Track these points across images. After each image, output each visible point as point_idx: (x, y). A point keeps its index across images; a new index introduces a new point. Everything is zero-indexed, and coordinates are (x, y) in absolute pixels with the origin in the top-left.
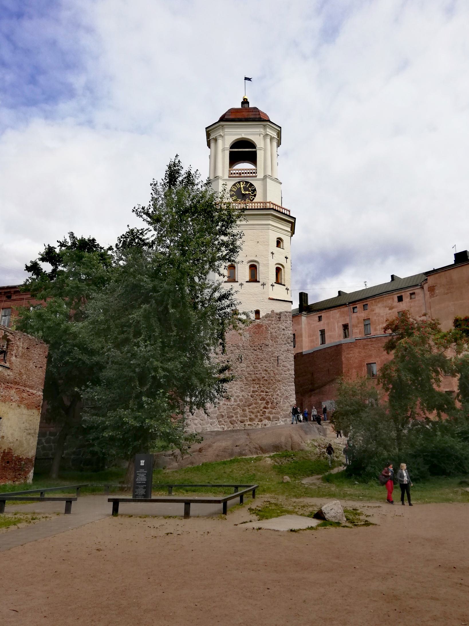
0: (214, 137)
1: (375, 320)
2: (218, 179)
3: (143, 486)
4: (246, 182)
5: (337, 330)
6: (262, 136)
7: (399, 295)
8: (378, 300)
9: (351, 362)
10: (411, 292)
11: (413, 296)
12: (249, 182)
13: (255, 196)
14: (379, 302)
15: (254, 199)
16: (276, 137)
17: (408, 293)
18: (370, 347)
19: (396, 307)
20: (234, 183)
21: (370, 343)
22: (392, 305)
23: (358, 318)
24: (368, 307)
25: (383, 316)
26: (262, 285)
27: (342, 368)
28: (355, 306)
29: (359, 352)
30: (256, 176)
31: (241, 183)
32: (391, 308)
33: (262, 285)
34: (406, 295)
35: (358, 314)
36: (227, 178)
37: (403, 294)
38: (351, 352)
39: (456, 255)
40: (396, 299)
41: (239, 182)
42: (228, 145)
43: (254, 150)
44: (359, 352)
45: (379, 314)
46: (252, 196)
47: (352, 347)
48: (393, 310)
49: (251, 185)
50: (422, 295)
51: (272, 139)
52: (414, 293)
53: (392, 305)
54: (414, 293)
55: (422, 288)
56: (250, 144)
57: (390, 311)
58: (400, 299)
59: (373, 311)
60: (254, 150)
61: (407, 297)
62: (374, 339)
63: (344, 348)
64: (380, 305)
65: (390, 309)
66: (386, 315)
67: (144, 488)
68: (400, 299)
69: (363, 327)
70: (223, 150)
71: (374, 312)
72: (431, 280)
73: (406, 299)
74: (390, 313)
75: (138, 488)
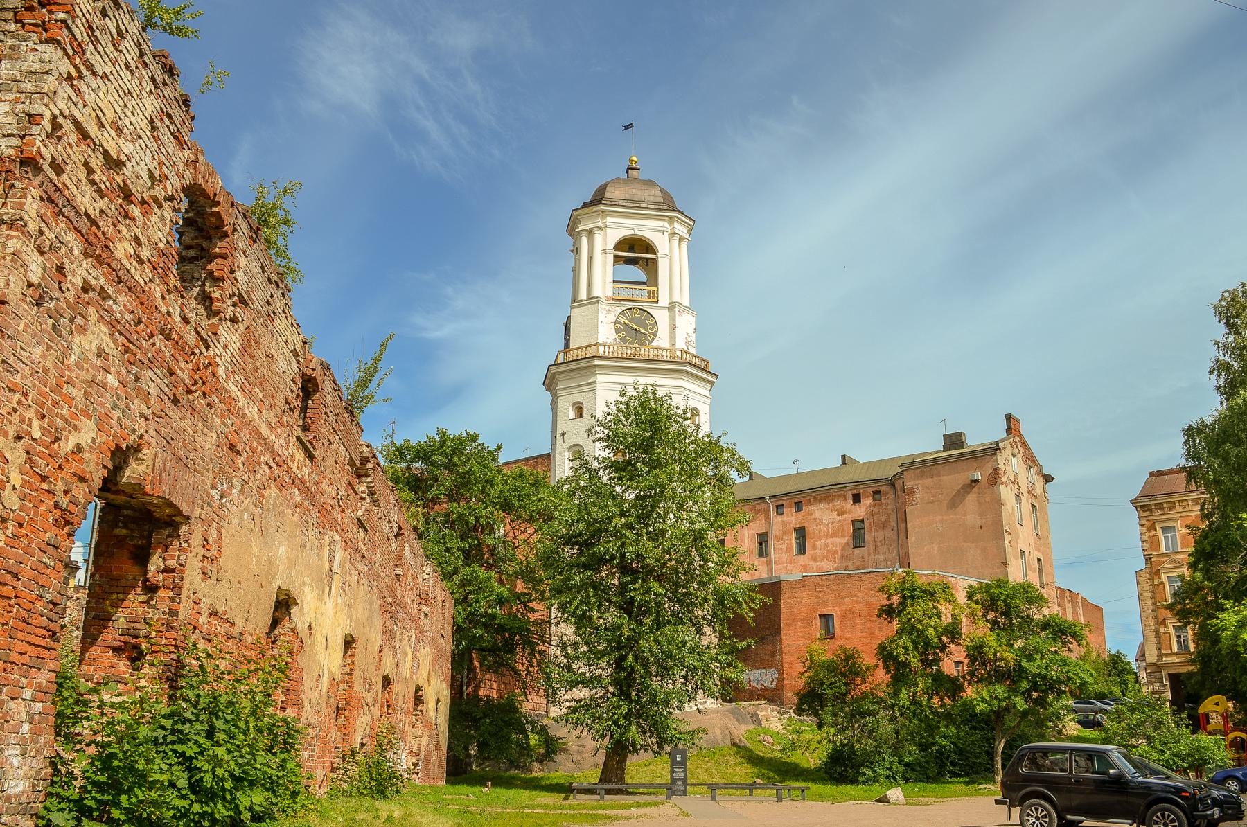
0: (588, 227)
2: (597, 302)
3: (681, 781)
4: (640, 309)
5: (746, 541)
6: (666, 234)
7: (855, 492)
9: (795, 610)
10: (875, 489)
11: (877, 496)
12: (645, 311)
13: (655, 334)
15: (653, 339)
16: (687, 236)
17: (870, 491)
18: (825, 588)
19: (848, 512)
21: (825, 583)
22: (843, 507)
23: (784, 524)
27: (780, 620)
28: (780, 503)
29: (808, 596)
32: (841, 513)
35: (785, 518)
38: (796, 595)
40: (850, 501)
42: (611, 245)
43: (654, 256)
44: (808, 596)
45: (821, 521)
47: (798, 588)
51: (681, 239)
56: (648, 247)
59: (811, 514)
60: (654, 256)
61: (868, 497)
62: (832, 578)
63: (784, 587)
64: (822, 506)
65: (838, 515)
67: (683, 783)
68: (857, 499)
70: (604, 252)
71: (813, 517)
74: (840, 521)
75: (675, 783)
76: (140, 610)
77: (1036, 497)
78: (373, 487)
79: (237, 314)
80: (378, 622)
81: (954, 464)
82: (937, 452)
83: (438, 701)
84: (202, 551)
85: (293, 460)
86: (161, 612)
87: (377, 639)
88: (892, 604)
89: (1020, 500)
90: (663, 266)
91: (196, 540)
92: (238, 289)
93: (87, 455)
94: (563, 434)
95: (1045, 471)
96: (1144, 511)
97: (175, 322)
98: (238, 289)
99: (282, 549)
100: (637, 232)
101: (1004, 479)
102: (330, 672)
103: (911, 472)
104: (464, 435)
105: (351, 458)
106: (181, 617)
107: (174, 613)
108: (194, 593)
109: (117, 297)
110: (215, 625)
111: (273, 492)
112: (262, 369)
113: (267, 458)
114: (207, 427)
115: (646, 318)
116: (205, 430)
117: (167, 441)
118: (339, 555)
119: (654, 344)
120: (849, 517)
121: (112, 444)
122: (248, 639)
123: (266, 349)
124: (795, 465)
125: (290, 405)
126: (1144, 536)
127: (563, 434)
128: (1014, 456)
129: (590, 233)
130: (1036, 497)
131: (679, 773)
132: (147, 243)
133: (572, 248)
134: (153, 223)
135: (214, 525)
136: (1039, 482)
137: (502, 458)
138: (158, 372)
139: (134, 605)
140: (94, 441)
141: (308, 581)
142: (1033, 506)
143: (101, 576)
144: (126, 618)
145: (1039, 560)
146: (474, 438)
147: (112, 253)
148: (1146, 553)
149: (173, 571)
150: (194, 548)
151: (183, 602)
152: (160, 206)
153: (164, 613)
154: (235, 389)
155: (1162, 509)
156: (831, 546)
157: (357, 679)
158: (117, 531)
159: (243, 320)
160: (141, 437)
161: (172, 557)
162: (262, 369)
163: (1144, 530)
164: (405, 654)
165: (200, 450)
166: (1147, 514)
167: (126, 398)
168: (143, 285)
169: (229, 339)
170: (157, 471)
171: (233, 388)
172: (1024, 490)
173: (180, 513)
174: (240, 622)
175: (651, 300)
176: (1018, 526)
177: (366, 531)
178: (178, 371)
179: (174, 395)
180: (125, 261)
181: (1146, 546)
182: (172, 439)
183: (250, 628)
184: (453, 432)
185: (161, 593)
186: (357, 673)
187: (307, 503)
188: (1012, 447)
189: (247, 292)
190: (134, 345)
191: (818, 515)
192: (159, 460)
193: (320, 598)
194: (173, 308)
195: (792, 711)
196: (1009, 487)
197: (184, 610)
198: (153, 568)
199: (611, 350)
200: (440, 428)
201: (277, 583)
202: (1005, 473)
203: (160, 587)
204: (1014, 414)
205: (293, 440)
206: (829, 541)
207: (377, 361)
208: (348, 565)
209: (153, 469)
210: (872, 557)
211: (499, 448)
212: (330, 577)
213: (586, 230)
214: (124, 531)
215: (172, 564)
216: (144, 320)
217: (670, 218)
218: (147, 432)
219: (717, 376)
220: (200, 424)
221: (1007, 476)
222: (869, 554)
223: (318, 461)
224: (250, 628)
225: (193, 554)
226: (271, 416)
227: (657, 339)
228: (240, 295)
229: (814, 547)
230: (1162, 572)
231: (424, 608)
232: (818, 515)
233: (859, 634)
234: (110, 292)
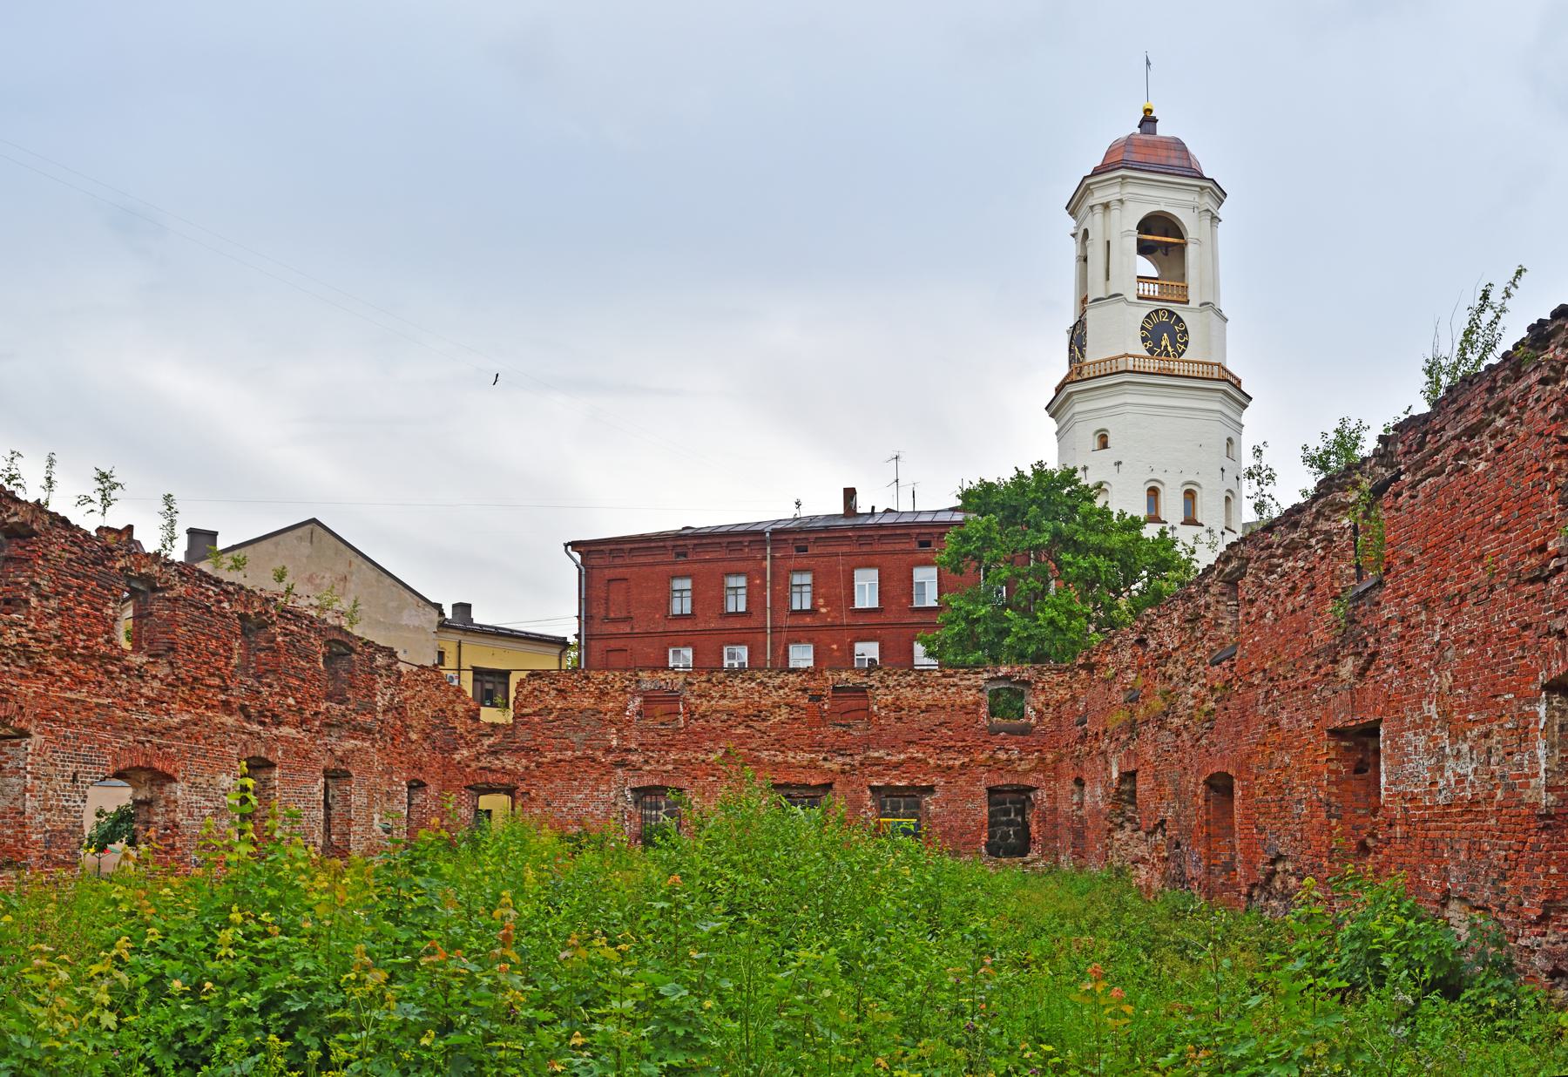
4: (1168, 311)
12: (1174, 313)
13: (1186, 344)
15: (1183, 351)
20: (1147, 311)
26: (1207, 531)
30: (1187, 302)
31: (1161, 313)
33: (1207, 531)
36: (1136, 300)
41: (1156, 311)
43: (1181, 241)
46: (1182, 344)
49: (1179, 320)
133: (1073, 231)
217: (1202, 188)
219: (1251, 399)
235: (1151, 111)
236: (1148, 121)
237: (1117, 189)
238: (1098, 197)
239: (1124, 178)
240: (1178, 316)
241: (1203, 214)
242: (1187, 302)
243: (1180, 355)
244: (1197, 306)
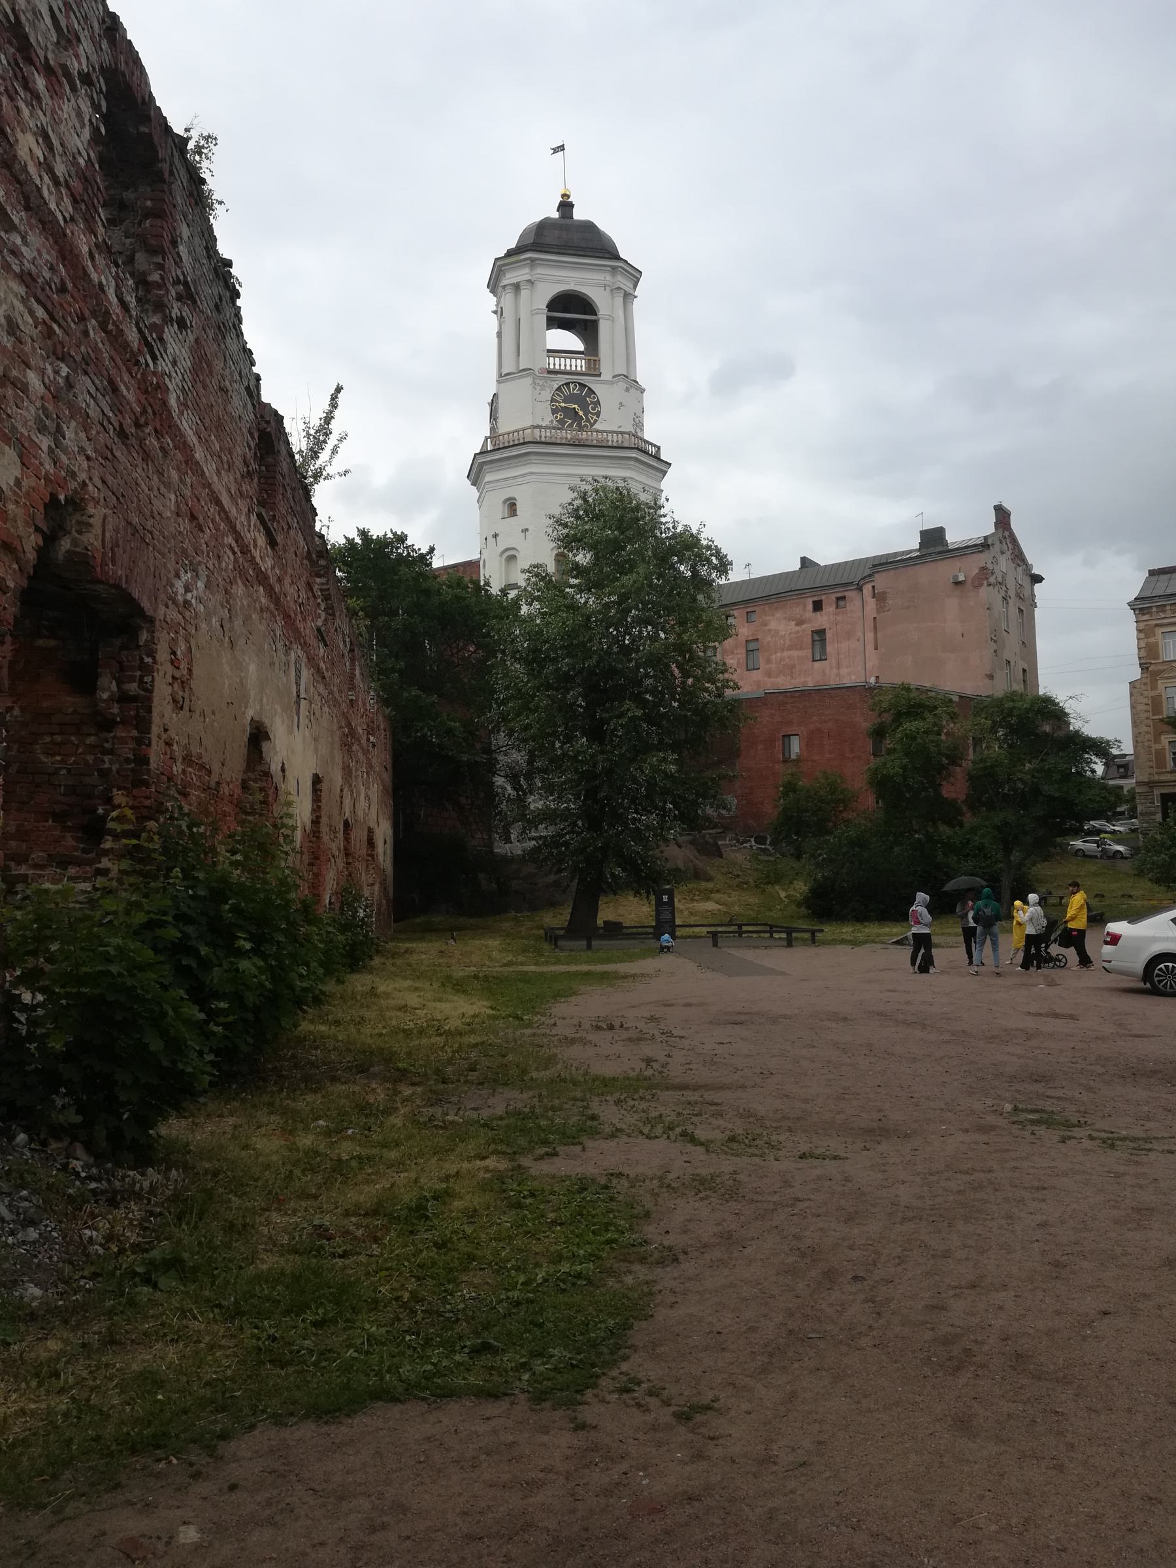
0: (515, 281)
1: (769, 643)
4: (580, 384)
7: (816, 599)
8: (775, 605)
9: (756, 731)
10: (839, 595)
11: (841, 603)
12: (586, 386)
13: (598, 414)
14: (777, 608)
15: (596, 421)
17: (833, 597)
18: (789, 706)
22: (801, 616)
24: (754, 617)
25: (783, 637)
30: (599, 375)
31: (572, 386)
34: (829, 600)
37: (823, 597)
39: (924, 534)
40: (810, 607)
41: (567, 384)
42: (543, 305)
43: (593, 318)
45: (777, 632)
46: (593, 414)
48: (804, 626)
49: (591, 391)
50: (858, 603)
52: (844, 598)
53: (801, 616)
54: (844, 598)
55: (860, 589)
57: (797, 628)
58: (818, 606)
59: (766, 625)
60: (593, 318)
65: (797, 624)
66: (790, 633)
68: (818, 606)
69: (744, 655)
70: (534, 313)
71: (767, 628)
72: (881, 581)
73: (829, 608)
74: (798, 632)
76: (90, 758)
77: (1023, 600)
78: (328, 589)
79: (184, 314)
80: (338, 758)
81: (918, 566)
82: (911, 551)
83: (385, 842)
84: (170, 669)
85: (255, 546)
86: (122, 759)
87: (338, 780)
88: (883, 722)
89: (1007, 603)
90: (604, 329)
91: (163, 655)
92: (183, 273)
93: (11, 507)
94: (496, 536)
95: (1035, 571)
96: (1144, 614)
97: (110, 303)
98: (183, 273)
99: (252, 668)
100: (572, 286)
101: (992, 580)
102: (302, 822)
103: (884, 574)
104: (390, 535)
105: (309, 552)
106: (153, 765)
107: (143, 760)
108: (166, 730)
109: (26, 233)
110: (190, 773)
111: (239, 590)
112: (217, 407)
113: (230, 540)
114: (163, 483)
115: (588, 395)
116: (163, 489)
117: (118, 499)
118: (305, 673)
119: (597, 426)
120: (808, 628)
121: (45, 491)
122: (225, 790)
123: (220, 377)
124: (747, 570)
125: (248, 467)
126: (1141, 642)
127: (496, 536)
128: (1002, 553)
129: (517, 287)
130: (1023, 600)
131: (666, 915)
132: (60, 149)
133: (494, 308)
134: (66, 116)
135: (182, 631)
136: (1026, 581)
137: (437, 563)
138: (97, 381)
139: (80, 750)
140: (18, 482)
141: (279, 710)
142: (1021, 611)
143: (22, 709)
144: (69, 770)
145: (1024, 671)
146: (402, 538)
147: (11, 146)
148: (1143, 661)
149: (134, 699)
150: (162, 664)
151: (154, 743)
152: (74, 89)
153: (127, 761)
154: (191, 433)
155: (1164, 611)
156: (787, 660)
157: (324, 829)
158: (40, 642)
159: (192, 326)
160: (84, 484)
161: (132, 679)
162: (217, 407)
163: (1142, 635)
164: (359, 793)
165: (158, 517)
166: (1146, 617)
167: (58, 417)
168: (62, 223)
169: (178, 352)
170: (108, 545)
171: (187, 428)
172: (1012, 593)
173: (140, 611)
174: (216, 768)
175: (592, 372)
176: (1005, 633)
177: (326, 645)
178: (123, 387)
179: (121, 425)
180: (32, 169)
181: (1143, 654)
182: (123, 496)
183: (227, 776)
184: (376, 532)
185: (120, 732)
186: (324, 820)
187: (272, 606)
188: (1001, 542)
189: (194, 281)
190: (60, 326)
191: (773, 625)
192: (109, 527)
193: (290, 731)
194: (107, 279)
195: (753, 840)
196: (996, 588)
197: (156, 753)
198: (105, 696)
199: (548, 434)
200: (361, 528)
201: (250, 713)
202: (993, 573)
203: (118, 723)
204: (1006, 505)
205: (254, 518)
206: (786, 654)
207: (328, 419)
208: (312, 689)
209: (103, 540)
210: (835, 671)
211: (432, 550)
212: (298, 703)
213: (513, 284)
214: (52, 643)
215: (133, 688)
216: (70, 286)
217: (614, 268)
218: (90, 479)
219: (670, 464)
220: (155, 478)
221: (994, 576)
222: (831, 668)
223: (279, 548)
224: (227, 776)
225: (161, 674)
226: (229, 478)
227: (600, 420)
228: (186, 284)
229: (769, 661)
230: (1159, 682)
231: (372, 738)
232: (773, 625)
233: (828, 756)
234: (16, 220)
235: (568, 197)
236: (566, 206)
237: (527, 270)
238: (510, 278)
239: (533, 260)
240: (589, 388)
241: (615, 291)
242: (599, 375)
243: (592, 425)
244: (610, 379)
